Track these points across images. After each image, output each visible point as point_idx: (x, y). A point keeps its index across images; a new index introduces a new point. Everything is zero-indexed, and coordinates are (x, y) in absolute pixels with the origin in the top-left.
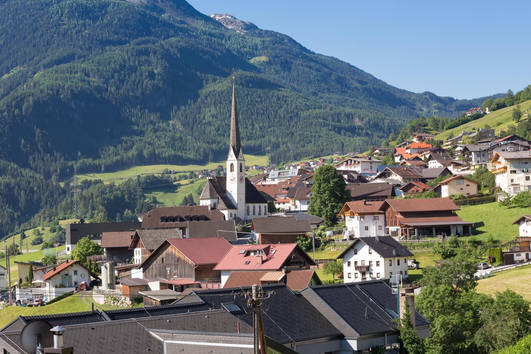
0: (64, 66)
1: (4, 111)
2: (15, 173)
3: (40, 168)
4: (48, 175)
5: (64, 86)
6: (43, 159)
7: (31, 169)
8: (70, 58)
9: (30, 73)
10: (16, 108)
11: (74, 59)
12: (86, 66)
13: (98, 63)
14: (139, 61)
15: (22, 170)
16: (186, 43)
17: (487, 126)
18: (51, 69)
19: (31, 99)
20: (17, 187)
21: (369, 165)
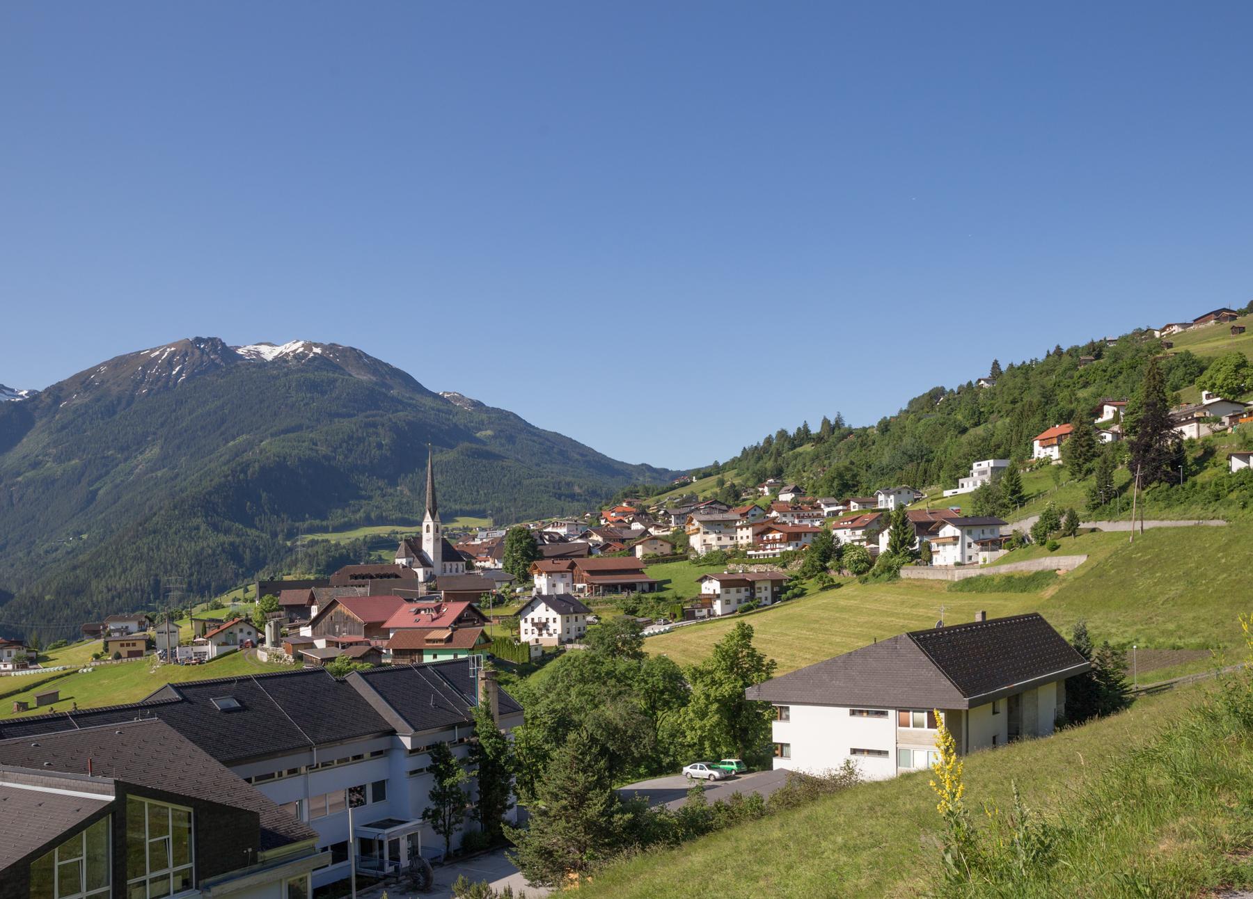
0: (291, 435)
1: (229, 475)
4: (274, 535)
6: (270, 521)
7: (257, 529)
8: (299, 428)
10: (241, 473)
11: (302, 430)
12: (314, 436)
14: (367, 433)
15: (248, 530)
17: (692, 493)
18: (278, 438)
19: (257, 465)
20: (242, 546)
21: (575, 527)
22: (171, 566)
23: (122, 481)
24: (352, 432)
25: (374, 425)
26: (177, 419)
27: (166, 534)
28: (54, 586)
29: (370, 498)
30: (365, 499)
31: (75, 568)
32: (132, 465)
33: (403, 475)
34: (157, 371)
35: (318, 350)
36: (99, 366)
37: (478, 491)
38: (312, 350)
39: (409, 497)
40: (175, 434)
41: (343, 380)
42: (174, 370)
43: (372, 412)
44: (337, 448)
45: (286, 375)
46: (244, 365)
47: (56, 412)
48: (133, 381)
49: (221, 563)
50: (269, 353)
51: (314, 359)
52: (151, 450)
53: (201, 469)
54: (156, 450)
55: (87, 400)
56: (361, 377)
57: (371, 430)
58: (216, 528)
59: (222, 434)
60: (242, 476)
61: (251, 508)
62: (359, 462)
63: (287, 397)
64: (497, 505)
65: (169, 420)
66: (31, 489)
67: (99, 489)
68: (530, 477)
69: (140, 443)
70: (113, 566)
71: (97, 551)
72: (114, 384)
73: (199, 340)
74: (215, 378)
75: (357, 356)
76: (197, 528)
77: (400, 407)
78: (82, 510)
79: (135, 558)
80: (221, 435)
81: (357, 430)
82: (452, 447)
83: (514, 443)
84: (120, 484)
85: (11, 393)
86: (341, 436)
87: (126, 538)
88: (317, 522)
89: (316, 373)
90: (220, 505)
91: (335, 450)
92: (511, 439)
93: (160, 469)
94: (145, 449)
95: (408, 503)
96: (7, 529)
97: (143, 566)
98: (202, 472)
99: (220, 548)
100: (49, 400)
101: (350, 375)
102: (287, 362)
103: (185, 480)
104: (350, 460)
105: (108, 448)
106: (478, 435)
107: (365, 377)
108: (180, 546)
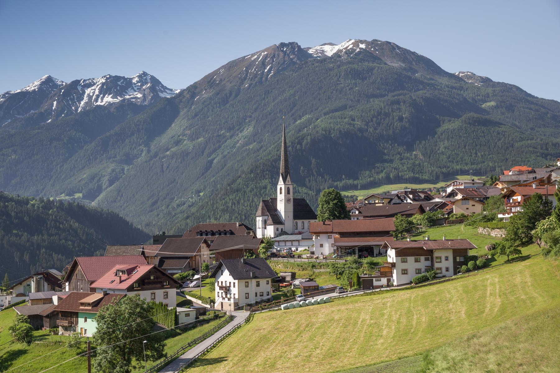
0: (337, 114)
3: (313, 187)
5: (334, 128)
6: (316, 181)
7: (307, 187)
8: (344, 107)
9: (314, 119)
13: (362, 111)
15: (300, 188)
16: (430, 94)
18: (327, 116)
22: (245, 216)
23: (228, 153)
24: (381, 109)
25: (398, 102)
26: (265, 105)
27: (245, 192)
29: (391, 161)
31: (187, 218)
33: (418, 142)
34: (255, 70)
35: (363, 46)
36: (219, 69)
37: (476, 154)
39: (421, 160)
40: (263, 116)
41: (379, 68)
42: (265, 69)
44: (369, 122)
45: (339, 66)
47: (192, 104)
48: (239, 78)
50: (330, 51)
51: (360, 53)
52: (248, 129)
53: (276, 142)
54: (251, 129)
55: (211, 94)
56: (393, 65)
57: (395, 107)
59: (293, 115)
60: (298, 147)
61: (303, 172)
63: (338, 84)
64: (491, 164)
65: (260, 107)
66: (174, 160)
67: (214, 159)
68: (522, 139)
69: (241, 124)
70: (209, 216)
71: (202, 205)
72: (228, 81)
73: (283, 45)
74: (291, 72)
75: (390, 47)
76: (265, 187)
77: (421, 87)
78: (203, 174)
79: (223, 210)
80: (292, 116)
81: (385, 107)
82: (458, 117)
83: (513, 111)
84: (226, 155)
85: (170, 92)
86: (372, 112)
87: (220, 195)
88: (351, 181)
89: (360, 64)
91: (367, 124)
92: (510, 108)
93: (252, 143)
94: (244, 129)
95: (420, 164)
96: (159, 189)
98: (276, 144)
100: (188, 96)
101: (386, 64)
103: (265, 151)
104: (377, 131)
105: (221, 129)
106: (483, 106)
107: (396, 64)
108: (253, 201)
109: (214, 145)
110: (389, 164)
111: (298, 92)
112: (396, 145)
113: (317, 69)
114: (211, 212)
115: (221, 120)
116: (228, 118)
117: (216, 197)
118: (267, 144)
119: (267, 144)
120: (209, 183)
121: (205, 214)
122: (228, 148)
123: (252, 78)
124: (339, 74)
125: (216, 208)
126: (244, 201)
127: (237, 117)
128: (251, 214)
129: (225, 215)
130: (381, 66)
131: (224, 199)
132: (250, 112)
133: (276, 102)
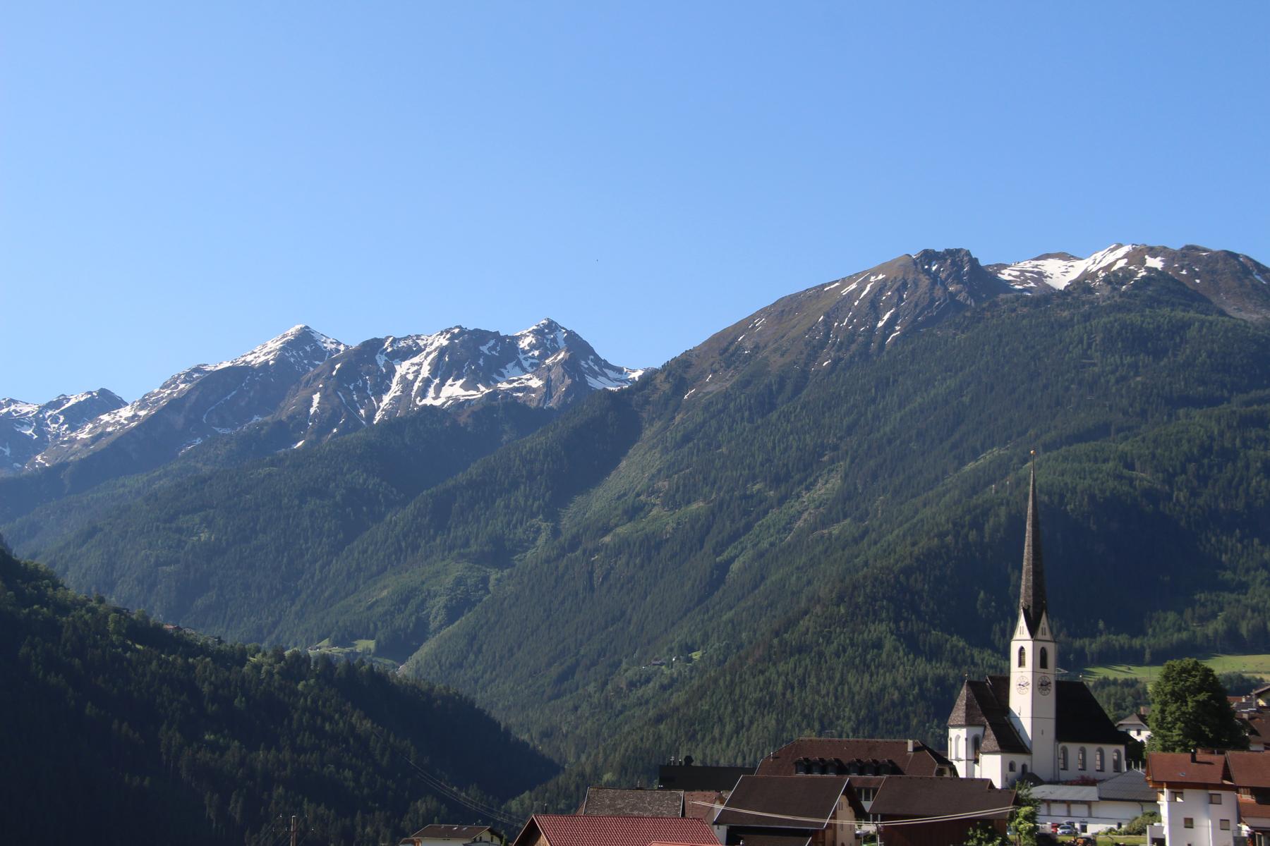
0: (1082, 447)
1: (946, 534)
2: (959, 658)
5: (1075, 488)
8: (1101, 431)
9: (1015, 460)
13: (1155, 441)
15: (976, 652)
18: (1055, 453)
23: (772, 544)
24: (1211, 438)
27: (821, 654)
28: (617, 758)
29: (1242, 587)
30: (1232, 591)
31: (659, 719)
32: (792, 511)
34: (851, 321)
35: (1156, 263)
36: (752, 318)
38: (1144, 261)
40: (869, 448)
42: (878, 319)
43: (1260, 393)
45: (1087, 318)
46: (1006, 301)
47: (676, 409)
48: (807, 344)
49: (914, 722)
50: (1060, 275)
52: (827, 482)
53: (907, 520)
55: (728, 385)
57: (1253, 433)
58: (913, 645)
59: (954, 446)
60: (973, 535)
62: (1222, 505)
63: (1083, 366)
66: (624, 559)
67: (731, 560)
70: (720, 719)
72: (775, 351)
73: (929, 256)
74: (952, 331)
76: (878, 645)
78: (700, 601)
79: (760, 704)
81: (1222, 434)
84: (767, 550)
87: (750, 662)
88: (1122, 640)
89: (1147, 311)
90: (925, 595)
91: (1170, 479)
93: (838, 521)
94: (816, 481)
97: (771, 721)
98: (906, 526)
99: (916, 690)
100: (666, 387)
102: (1090, 290)
103: (875, 543)
104: (1201, 501)
105: (754, 479)
108: (843, 681)
109: (733, 521)
110: (1234, 596)
111: (969, 384)
112: (1256, 541)
113: (1024, 322)
114: (726, 708)
115: (753, 456)
116: (774, 448)
117: (741, 666)
118: (881, 525)
119: (881, 525)
120: (719, 626)
121: (709, 711)
122: (772, 531)
123: (841, 343)
124: (1089, 338)
125: (741, 697)
126: (819, 681)
127: (798, 449)
128: (838, 718)
129: (766, 718)
130: (1210, 318)
131: (762, 672)
132: (835, 435)
133: (907, 409)
